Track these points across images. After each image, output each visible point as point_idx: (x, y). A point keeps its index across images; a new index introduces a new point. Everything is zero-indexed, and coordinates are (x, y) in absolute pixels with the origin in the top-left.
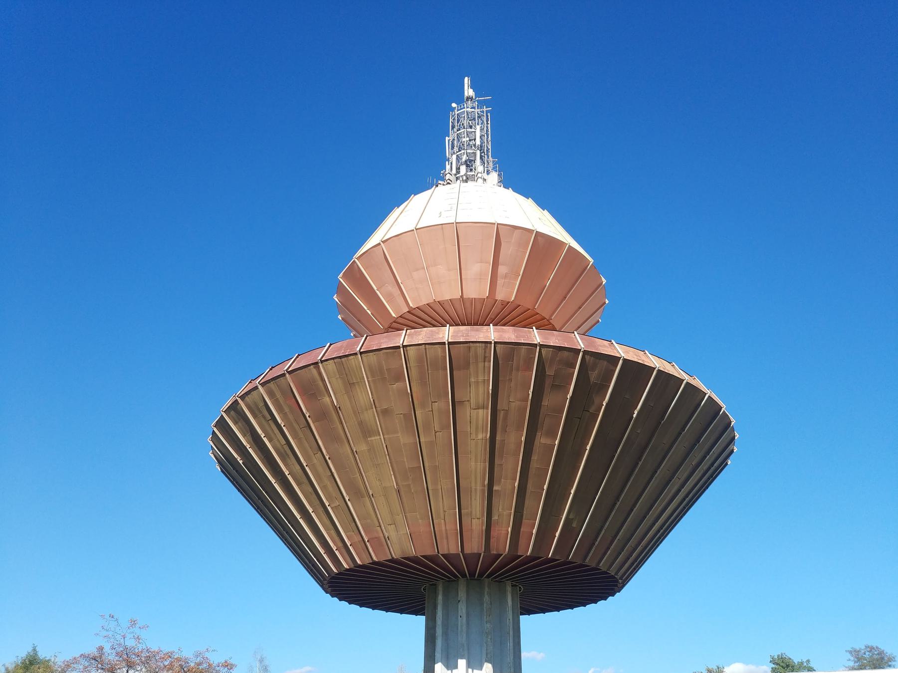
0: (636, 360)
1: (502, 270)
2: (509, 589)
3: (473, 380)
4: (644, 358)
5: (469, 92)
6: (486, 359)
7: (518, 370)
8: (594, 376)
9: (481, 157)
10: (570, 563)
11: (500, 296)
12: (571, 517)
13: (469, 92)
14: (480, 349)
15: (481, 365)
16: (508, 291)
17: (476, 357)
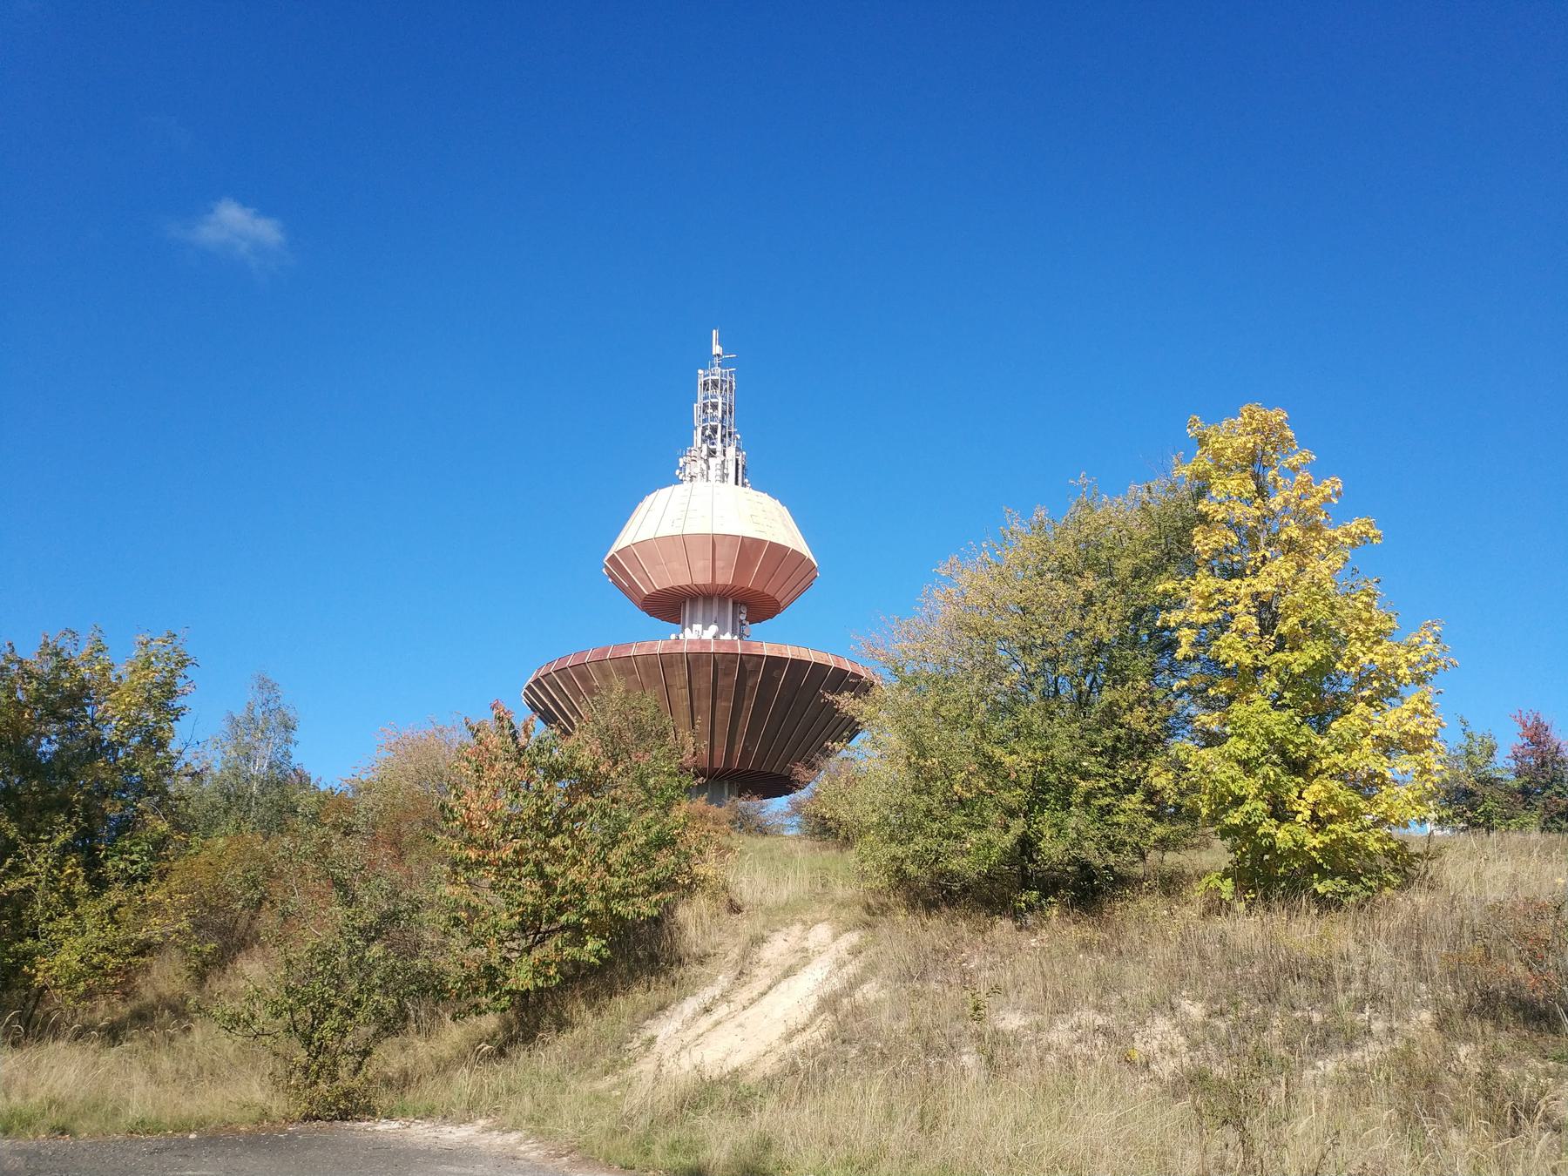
0: (780, 655)
1: (719, 564)
2: (726, 785)
3: (676, 673)
4: (784, 651)
5: (717, 349)
6: (682, 662)
7: (702, 667)
8: (749, 667)
9: (723, 427)
10: (750, 771)
11: (720, 580)
12: (747, 744)
13: (717, 349)
14: (679, 656)
15: (680, 665)
16: (726, 578)
17: (677, 660)
